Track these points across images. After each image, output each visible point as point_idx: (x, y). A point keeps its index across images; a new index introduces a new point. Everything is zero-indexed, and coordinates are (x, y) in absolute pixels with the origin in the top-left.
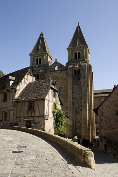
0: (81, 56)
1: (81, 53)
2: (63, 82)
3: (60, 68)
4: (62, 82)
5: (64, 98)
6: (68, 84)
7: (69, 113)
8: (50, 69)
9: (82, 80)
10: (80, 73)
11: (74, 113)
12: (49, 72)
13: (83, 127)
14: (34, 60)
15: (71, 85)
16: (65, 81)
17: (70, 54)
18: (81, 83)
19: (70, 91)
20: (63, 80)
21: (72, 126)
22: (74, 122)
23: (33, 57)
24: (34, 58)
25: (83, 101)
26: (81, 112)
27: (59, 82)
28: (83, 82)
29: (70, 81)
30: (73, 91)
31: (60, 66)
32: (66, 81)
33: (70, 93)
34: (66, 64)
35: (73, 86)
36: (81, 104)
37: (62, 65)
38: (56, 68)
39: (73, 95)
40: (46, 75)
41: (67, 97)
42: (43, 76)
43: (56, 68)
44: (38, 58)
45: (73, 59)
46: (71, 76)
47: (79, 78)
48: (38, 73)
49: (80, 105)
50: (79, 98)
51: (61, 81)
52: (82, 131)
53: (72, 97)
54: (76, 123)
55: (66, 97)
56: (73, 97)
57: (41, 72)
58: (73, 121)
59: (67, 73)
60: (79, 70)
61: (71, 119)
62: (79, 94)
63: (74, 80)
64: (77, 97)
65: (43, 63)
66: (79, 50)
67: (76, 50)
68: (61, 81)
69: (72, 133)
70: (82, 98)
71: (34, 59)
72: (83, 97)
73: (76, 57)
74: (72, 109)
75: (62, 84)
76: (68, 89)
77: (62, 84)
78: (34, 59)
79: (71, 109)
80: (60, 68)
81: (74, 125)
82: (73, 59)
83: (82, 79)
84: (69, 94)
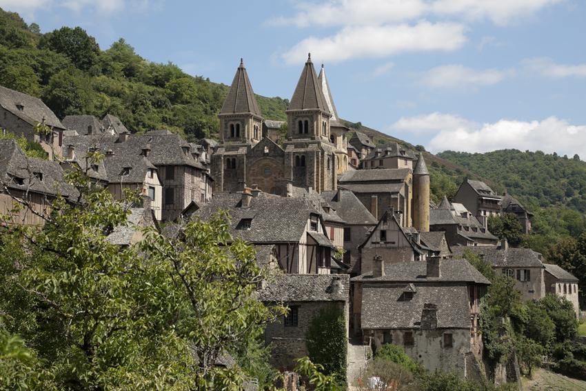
1: (309, 124)
9: (308, 179)
17: (291, 122)
44: (235, 124)
45: (296, 133)
66: (305, 117)
82: (296, 133)
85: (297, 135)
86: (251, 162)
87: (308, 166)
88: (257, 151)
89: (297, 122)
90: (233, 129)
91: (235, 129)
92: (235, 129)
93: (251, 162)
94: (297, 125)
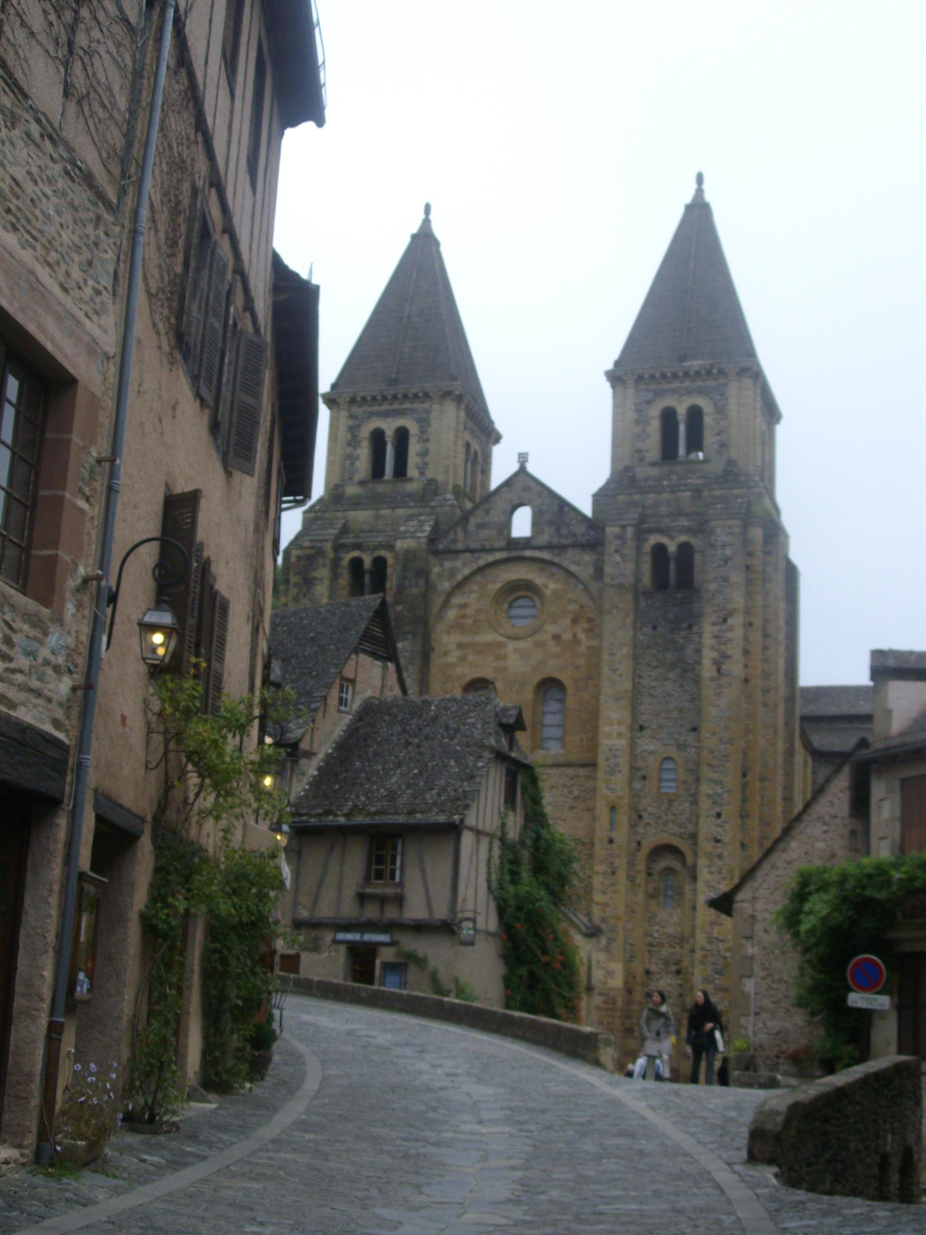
0: (710, 439)
1: (707, 420)
2: (567, 636)
3: (551, 523)
4: (556, 637)
5: (570, 771)
6: (605, 656)
7: (604, 893)
8: (471, 526)
9: (708, 640)
10: (698, 575)
11: (641, 897)
12: (467, 550)
14: (354, 442)
15: (625, 668)
16: (582, 636)
17: (631, 415)
18: (699, 663)
19: (614, 716)
20: (567, 621)
22: (638, 968)
23: (352, 416)
24: (359, 426)
25: (705, 805)
27: (538, 637)
28: (715, 654)
29: (618, 633)
30: (634, 712)
31: (553, 509)
32: (593, 629)
34: (599, 498)
35: (636, 676)
36: (691, 828)
37: (563, 505)
38: (522, 524)
39: (633, 745)
40: (440, 576)
41: (593, 765)
42: (421, 582)
43: (522, 524)
44: (389, 427)
46: (629, 597)
47: (688, 621)
48: (382, 553)
49: (681, 836)
51: (550, 629)
54: (648, 972)
55: (584, 765)
56: (633, 768)
57: (407, 552)
58: (629, 959)
59: (599, 572)
60: (686, 550)
61: (611, 941)
62: (681, 747)
63: (648, 630)
64: (668, 765)
65: (422, 474)
66: (689, 392)
67: (674, 391)
68: (550, 629)
70: (698, 780)
71: (354, 437)
72: (706, 771)
73: (668, 450)
74: (621, 863)
76: (602, 698)
78: (354, 431)
79: (617, 862)
80: (546, 529)
81: (638, 995)
83: (708, 630)
84: (605, 743)
85: (653, 464)
86: (453, 572)
87: (712, 586)
88: (480, 526)
89: (655, 412)
90: (384, 444)
91: (390, 450)
92: (390, 450)
93: (453, 572)
94: (655, 427)
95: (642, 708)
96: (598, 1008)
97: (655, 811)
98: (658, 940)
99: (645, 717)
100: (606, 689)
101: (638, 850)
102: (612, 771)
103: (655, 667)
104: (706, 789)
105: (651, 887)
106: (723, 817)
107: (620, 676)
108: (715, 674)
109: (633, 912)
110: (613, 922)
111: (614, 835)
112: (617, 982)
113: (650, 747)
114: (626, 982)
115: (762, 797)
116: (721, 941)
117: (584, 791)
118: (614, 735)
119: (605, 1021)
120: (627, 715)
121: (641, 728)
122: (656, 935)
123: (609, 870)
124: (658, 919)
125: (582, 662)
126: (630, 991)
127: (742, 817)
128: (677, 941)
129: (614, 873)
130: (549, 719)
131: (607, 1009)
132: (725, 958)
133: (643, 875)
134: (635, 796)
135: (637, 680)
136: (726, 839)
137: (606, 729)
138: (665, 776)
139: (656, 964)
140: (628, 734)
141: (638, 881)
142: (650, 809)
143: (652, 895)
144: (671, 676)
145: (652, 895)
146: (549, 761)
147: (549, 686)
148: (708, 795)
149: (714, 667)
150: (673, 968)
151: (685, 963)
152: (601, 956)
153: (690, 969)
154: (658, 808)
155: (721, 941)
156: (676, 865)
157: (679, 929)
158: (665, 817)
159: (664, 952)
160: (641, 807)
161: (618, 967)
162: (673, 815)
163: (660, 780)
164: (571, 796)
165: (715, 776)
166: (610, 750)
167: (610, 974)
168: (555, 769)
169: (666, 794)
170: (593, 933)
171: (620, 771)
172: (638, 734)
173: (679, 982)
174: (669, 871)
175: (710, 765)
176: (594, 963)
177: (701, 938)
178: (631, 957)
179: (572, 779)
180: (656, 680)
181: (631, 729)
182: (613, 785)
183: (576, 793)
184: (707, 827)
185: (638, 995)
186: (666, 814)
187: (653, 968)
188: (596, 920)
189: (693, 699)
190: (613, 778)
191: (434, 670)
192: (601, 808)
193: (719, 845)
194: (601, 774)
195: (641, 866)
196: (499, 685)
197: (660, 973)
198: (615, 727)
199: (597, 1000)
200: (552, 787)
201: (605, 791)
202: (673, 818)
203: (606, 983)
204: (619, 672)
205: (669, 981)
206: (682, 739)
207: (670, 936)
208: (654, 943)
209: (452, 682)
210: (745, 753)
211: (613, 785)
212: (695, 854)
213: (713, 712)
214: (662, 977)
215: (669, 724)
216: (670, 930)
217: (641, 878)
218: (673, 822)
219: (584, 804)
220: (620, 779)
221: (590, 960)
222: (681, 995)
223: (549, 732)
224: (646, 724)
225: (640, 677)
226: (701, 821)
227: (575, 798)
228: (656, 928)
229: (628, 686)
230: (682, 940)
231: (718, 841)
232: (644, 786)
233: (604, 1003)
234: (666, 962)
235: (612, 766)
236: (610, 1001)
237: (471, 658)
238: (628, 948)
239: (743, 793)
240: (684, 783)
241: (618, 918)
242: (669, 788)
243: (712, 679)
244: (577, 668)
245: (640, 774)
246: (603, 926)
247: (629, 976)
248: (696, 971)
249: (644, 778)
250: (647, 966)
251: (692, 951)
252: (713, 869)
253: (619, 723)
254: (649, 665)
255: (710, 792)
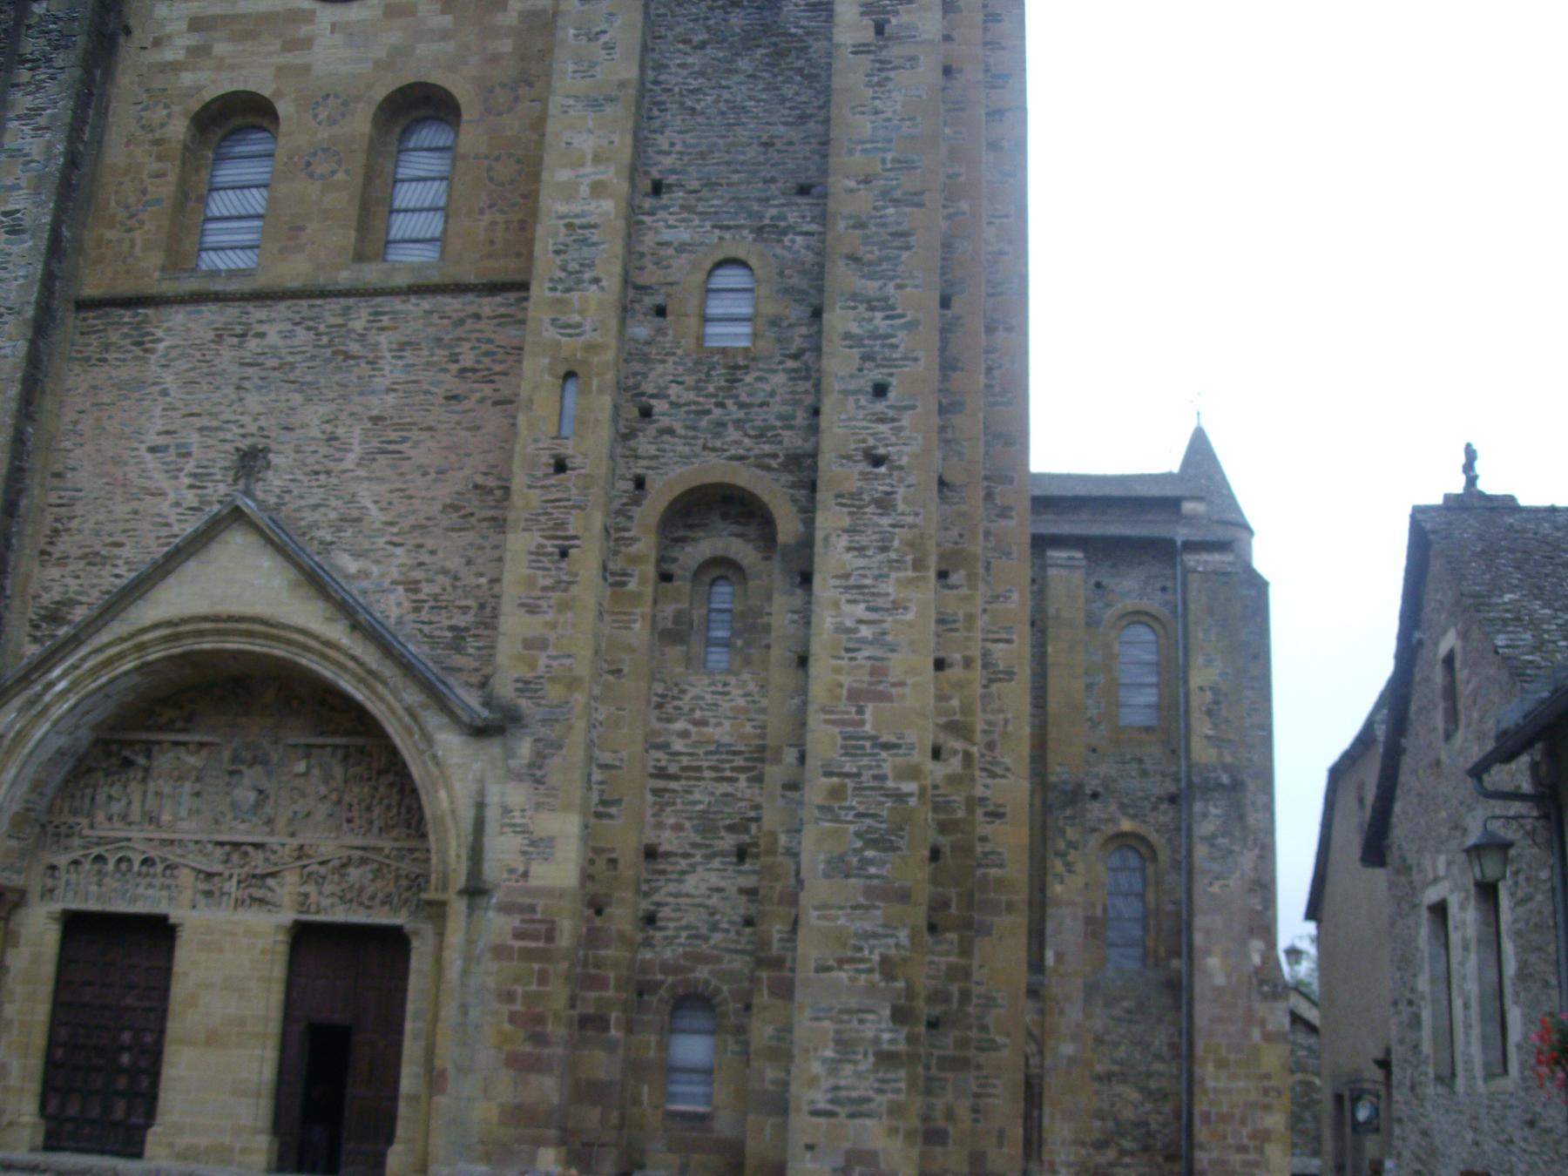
5: (452, 304)
7: (532, 610)
11: (639, 633)
13: (809, 951)
19: (586, 144)
21: (567, 931)
22: (625, 839)
25: (839, 364)
26: (781, 611)
30: (641, 143)
33: (583, 176)
36: (792, 441)
39: (633, 226)
50: (770, 309)
52: (782, 1054)
53: (612, 283)
54: (651, 853)
55: (493, 288)
58: (601, 810)
64: (730, 278)
69: (548, 1089)
72: (842, 276)
74: (589, 526)
75: (444, 35)
77: (444, 35)
79: (574, 525)
81: (621, 918)
84: (554, 207)
95: (663, 141)
96: (500, 952)
97: (691, 396)
98: (685, 761)
99: (668, 161)
100: (567, 80)
101: (636, 502)
102: (574, 280)
103: (702, 46)
104: (838, 320)
105: (669, 610)
106: (892, 394)
107: (609, 47)
108: (869, 35)
109: (617, 672)
110: (554, 693)
111: (568, 449)
112: (561, 871)
113: (684, 235)
114: (587, 877)
115: (989, 370)
116: (887, 746)
117: (487, 354)
118: (584, 190)
119: (519, 989)
120: (623, 144)
121: (657, 189)
122: (678, 745)
123: (551, 546)
124: (685, 702)
125: (506, 46)
126: (598, 907)
127: (942, 410)
128: (740, 762)
129: (564, 554)
130: (406, 195)
131: (527, 955)
132: (900, 797)
133: (650, 570)
134: (635, 355)
135: (651, 74)
136: (904, 454)
137: (564, 175)
138: (716, 307)
139: (678, 827)
140: (624, 187)
141: (632, 586)
142: (674, 390)
143: (672, 634)
144: (742, 64)
145: (672, 634)
146: (401, 280)
147: (418, 106)
148: (848, 336)
149: (868, 22)
150: (728, 841)
151: (772, 818)
152: (517, 795)
153: (783, 839)
154: (697, 389)
155: (887, 746)
156: (742, 550)
157: (748, 729)
158: (717, 412)
159: (703, 795)
160: (649, 388)
161: (565, 826)
162: (742, 406)
163: (705, 319)
164: (454, 367)
165: (871, 287)
166: (569, 226)
167: (539, 846)
168: (413, 300)
169: (724, 351)
170: (493, 726)
171: (596, 281)
172: (648, 203)
173: (750, 882)
174: (722, 568)
175: (854, 258)
176: (492, 814)
177: (823, 739)
178: (603, 803)
179: (461, 322)
180: (702, 73)
181: (635, 170)
182: (577, 311)
183: (468, 360)
184: (845, 423)
185: (621, 918)
186: (721, 405)
187: (668, 841)
188: (505, 688)
189: (804, 118)
190: (575, 295)
191: (126, 81)
192: (536, 372)
193: (883, 470)
194: (540, 290)
195: (645, 544)
196: (284, 108)
197: (686, 855)
198: (588, 169)
199: (498, 925)
200: (402, 346)
201: (551, 333)
202: (741, 414)
203: (525, 875)
204: (604, 38)
205: (714, 879)
206: (774, 211)
207: (720, 748)
208: (673, 769)
209: (166, 106)
210: (947, 246)
211: (577, 311)
212: (808, 513)
213: (865, 126)
214: (693, 868)
215: (735, 177)
216: (722, 732)
217: (642, 579)
218: (738, 424)
219: (487, 390)
220: (596, 302)
221: (480, 806)
222: (749, 922)
223: (401, 226)
224: (671, 179)
225: (660, 67)
226: (826, 408)
227: (463, 371)
228: (680, 725)
229: (631, 72)
230: (757, 758)
231: (878, 461)
232: (660, 331)
233: (519, 935)
234: (706, 825)
235: (574, 266)
236: (537, 930)
237: (220, 48)
238: (597, 775)
239: (943, 350)
240: (774, 322)
241: (573, 683)
242: (733, 336)
243: (860, 50)
244: (495, 59)
245: (649, 301)
246: (524, 704)
247: (598, 860)
248: (807, 842)
249: (661, 311)
250: (650, 836)
251: (793, 786)
252: (863, 540)
253: (597, 159)
254: (684, 42)
255: (854, 328)
